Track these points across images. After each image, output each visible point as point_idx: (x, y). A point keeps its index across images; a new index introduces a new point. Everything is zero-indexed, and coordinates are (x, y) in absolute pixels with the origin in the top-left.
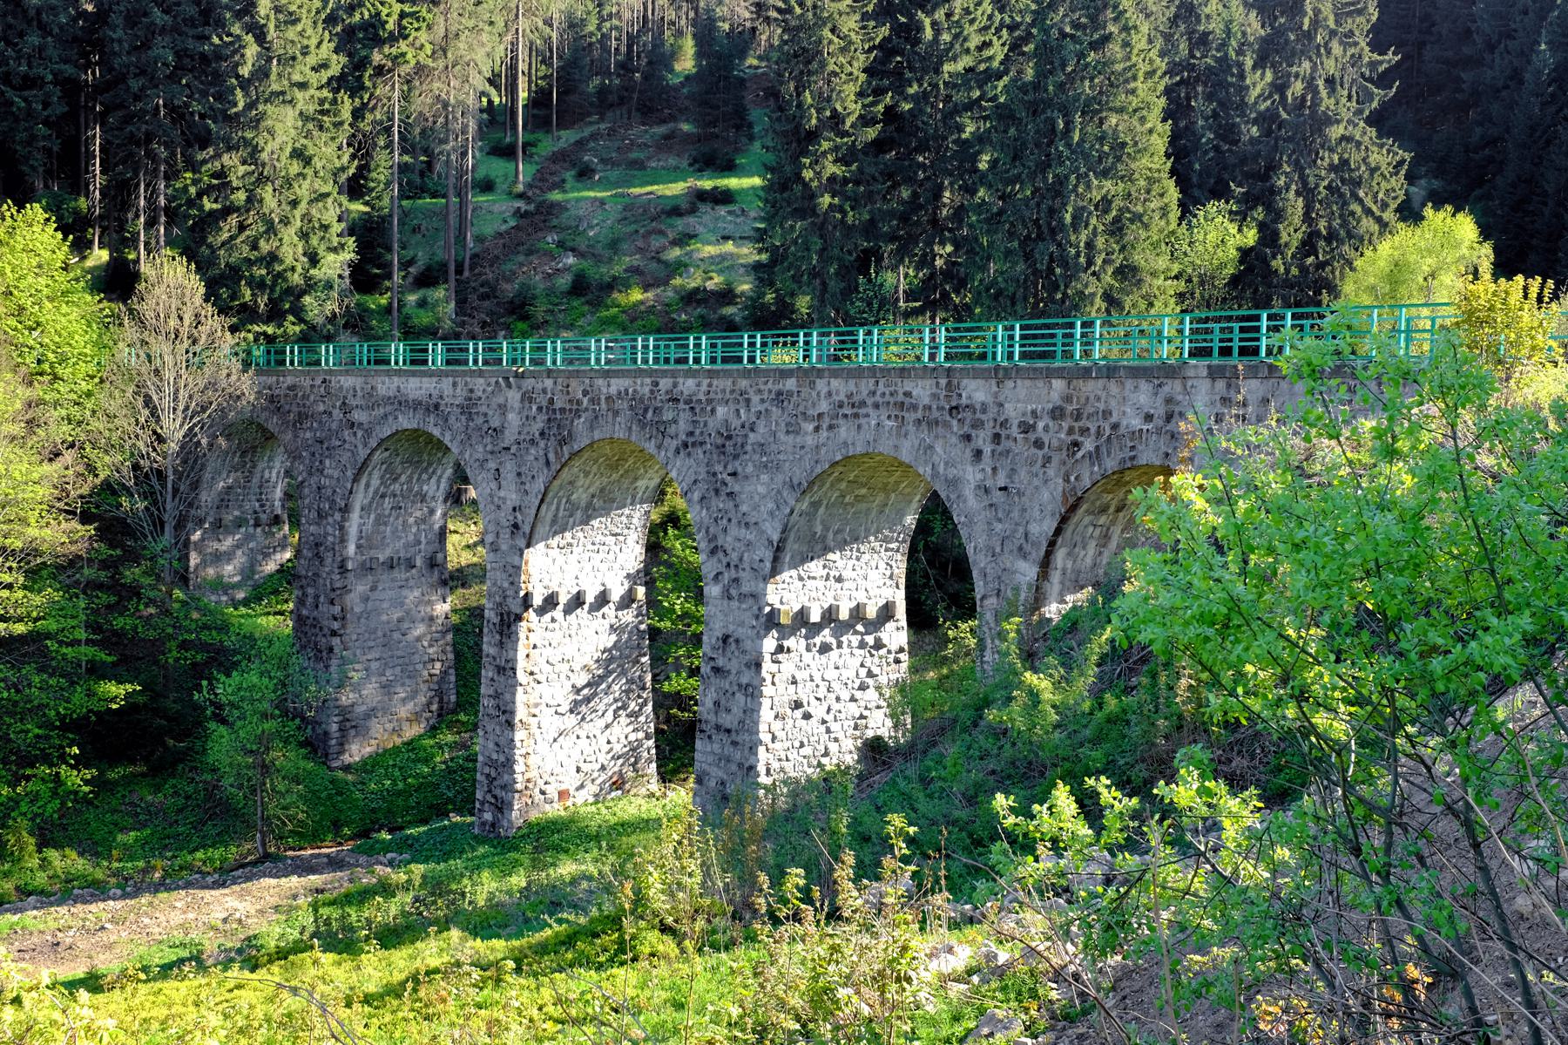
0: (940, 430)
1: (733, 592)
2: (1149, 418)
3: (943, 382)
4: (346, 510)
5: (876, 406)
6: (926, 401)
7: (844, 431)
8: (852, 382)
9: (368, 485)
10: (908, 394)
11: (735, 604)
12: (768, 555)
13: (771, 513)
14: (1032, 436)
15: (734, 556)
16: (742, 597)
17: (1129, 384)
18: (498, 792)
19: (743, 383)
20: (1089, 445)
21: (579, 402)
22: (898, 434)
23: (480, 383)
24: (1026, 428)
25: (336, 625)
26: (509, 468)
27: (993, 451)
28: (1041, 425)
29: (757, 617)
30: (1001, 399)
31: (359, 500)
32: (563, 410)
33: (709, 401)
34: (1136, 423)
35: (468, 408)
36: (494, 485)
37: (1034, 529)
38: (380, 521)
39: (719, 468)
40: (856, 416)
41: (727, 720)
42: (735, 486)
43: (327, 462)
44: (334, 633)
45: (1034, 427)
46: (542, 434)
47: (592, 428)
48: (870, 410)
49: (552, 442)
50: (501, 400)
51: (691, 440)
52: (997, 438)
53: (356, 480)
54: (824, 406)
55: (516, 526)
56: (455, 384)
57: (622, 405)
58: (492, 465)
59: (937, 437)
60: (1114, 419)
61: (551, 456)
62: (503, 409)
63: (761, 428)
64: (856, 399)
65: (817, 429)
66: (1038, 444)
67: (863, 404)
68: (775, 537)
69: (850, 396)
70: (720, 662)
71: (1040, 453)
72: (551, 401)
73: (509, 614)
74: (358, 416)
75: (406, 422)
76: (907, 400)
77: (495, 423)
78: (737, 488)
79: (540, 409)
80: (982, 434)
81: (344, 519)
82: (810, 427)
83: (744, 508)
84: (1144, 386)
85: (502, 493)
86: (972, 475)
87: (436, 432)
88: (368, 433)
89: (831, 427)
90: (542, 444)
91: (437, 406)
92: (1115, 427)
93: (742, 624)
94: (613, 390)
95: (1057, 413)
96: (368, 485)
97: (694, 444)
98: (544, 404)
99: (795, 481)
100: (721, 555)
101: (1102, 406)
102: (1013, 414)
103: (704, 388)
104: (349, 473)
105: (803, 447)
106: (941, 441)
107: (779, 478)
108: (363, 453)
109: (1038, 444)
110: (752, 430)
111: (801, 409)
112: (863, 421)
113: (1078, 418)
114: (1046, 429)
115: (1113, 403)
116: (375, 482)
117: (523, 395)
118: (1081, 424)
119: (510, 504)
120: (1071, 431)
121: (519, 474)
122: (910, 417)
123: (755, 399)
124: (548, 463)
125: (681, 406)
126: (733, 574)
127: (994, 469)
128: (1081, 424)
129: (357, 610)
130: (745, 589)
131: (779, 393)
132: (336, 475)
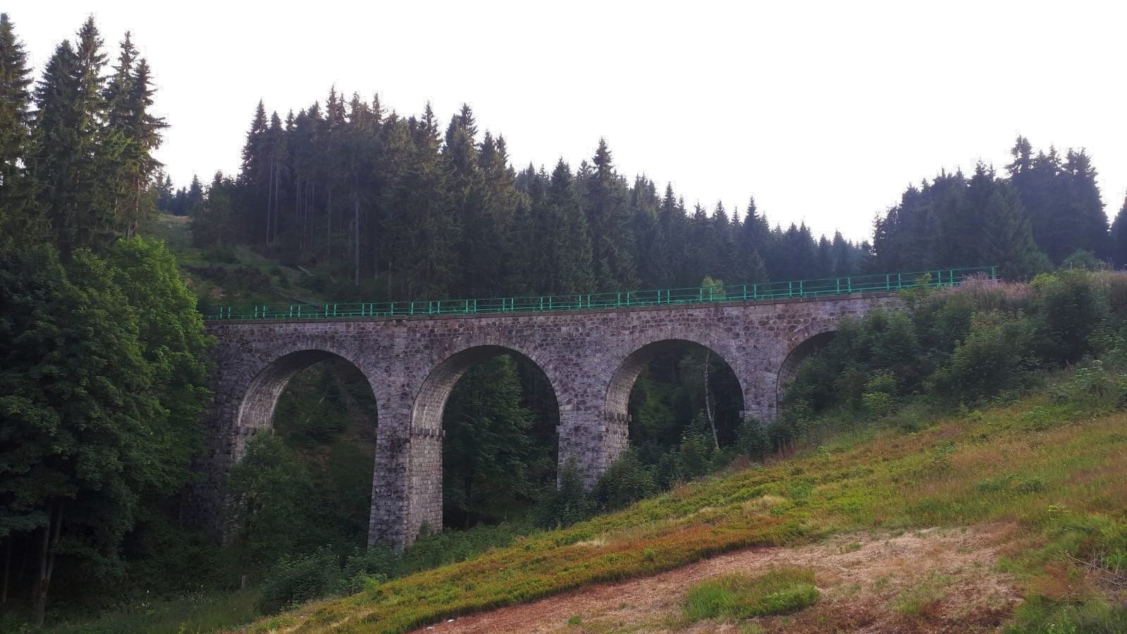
0: (713, 328)
1: (582, 407)
2: (832, 314)
3: (712, 309)
4: (240, 399)
6: (703, 317)
7: (650, 332)
11: (582, 412)
13: (604, 370)
14: (768, 326)
15: (581, 391)
17: (820, 303)
18: (390, 537)
20: (800, 327)
22: (687, 331)
23: (370, 326)
24: (763, 323)
26: (398, 366)
27: (745, 333)
28: (771, 322)
29: (598, 416)
30: (747, 313)
31: (249, 393)
33: (556, 325)
34: (826, 317)
35: (361, 337)
37: (773, 360)
38: (252, 408)
40: (659, 325)
43: (225, 372)
45: (767, 323)
47: (468, 342)
50: (389, 332)
51: (544, 343)
52: (747, 328)
53: (252, 381)
54: (636, 323)
56: (348, 326)
58: (383, 364)
59: (711, 330)
60: (813, 316)
61: (435, 357)
62: (392, 337)
63: (594, 335)
65: (631, 333)
66: (771, 329)
68: (608, 380)
71: (773, 332)
72: (432, 331)
73: (399, 440)
75: (302, 346)
78: (580, 361)
79: (423, 335)
80: (738, 327)
81: (240, 404)
84: (828, 303)
85: (392, 378)
86: (733, 343)
89: (641, 331)
90: (427, 352)
91: (333, 337)
92: (814, 319)
95: (779, 317)
96: (255, 385)
97: (547, 345)
98: (427, 332)
99: (620, 355)
100: (571, 391)
101: (806, 312)
102: (754, 319)
105: (623, 341)
106: (714, 332)
107: (608, 356)
108: (260, 366)
109: (771, 329)
110: (588, 336)
111: (621, 324)
113: (794, 317)
114: (775, 323)
115: (812, 311)
116: (258, 384)
117: (409, 329)
118: (795, 319)
119: (398, 384)
120: (789, 322)
121: (407, 368)
122: (693, 324)
124: (432, 362)
125: (536, 328)
126: (580, 398)
127: (747, 340)
128: (795, 319)
130: (588, 404)
131: (605, 319)
132: (234, 378)
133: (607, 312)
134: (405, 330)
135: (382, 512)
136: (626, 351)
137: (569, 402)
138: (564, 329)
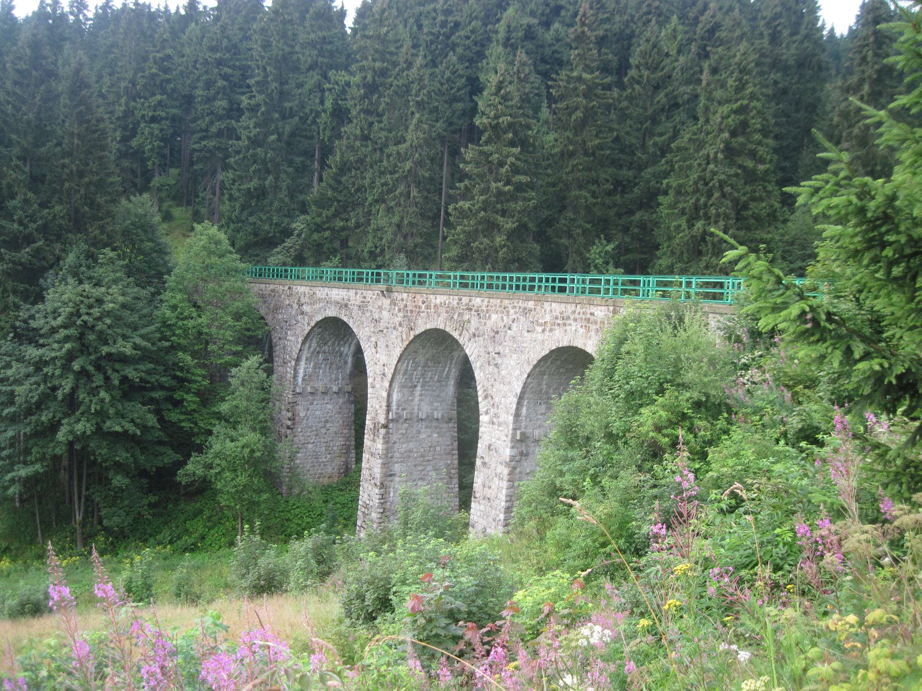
3: (611, 308)
5: (575, 320)
7: (558, 333)
8: (563, 305)
9: (310, 347)
10: (592, 314)
11: (496, 427)
12: (515, 400)
16: (500, 425)
19: (506, 302)
21: (420, 307)
25: (289, 423)
32: (412, 311)
36: (374, 350)
39: (491, 349)
40: (565, 325)
41: (488, 492)
42: (499, 361)
44: (288, 428)
46: (400, 325)
48: (572, 322)
49: (405, 329)
54: (548, 318)
55: (384, 374)
57: (442, 310)
58: (373, 339)
64: (565, 315)
65: (543, 331)
67: (568, 318)
68: (519, 391)
69: (561, 313)
70: (486, 460)
72: (406, 306)
74: (306, 308)
75: (331, 312)
76: (592, 318)
77: (376, 316)
79: (399, 310)
81: (296, 365)
82: (540, 329)
83: (503, 373)
87: (345, 319)
88: (311, 318)
89: (551, 330)
91: (346, 306)
93: (499, 439)
94: (438, 301)
96: (310, 347)
103: (485, 303)
104: (300, 340)
112: (568, 328)
116: (314, 345)
119: (381, 363)
123: (512, 311)
129: (302, 414)
130: (501, 419)
131: (525, 309)
133: (528, 299)
134: (389, 301)
135: (366, 496)
136: (535, 357)
137: (487, 413)
138: (494, 317)
